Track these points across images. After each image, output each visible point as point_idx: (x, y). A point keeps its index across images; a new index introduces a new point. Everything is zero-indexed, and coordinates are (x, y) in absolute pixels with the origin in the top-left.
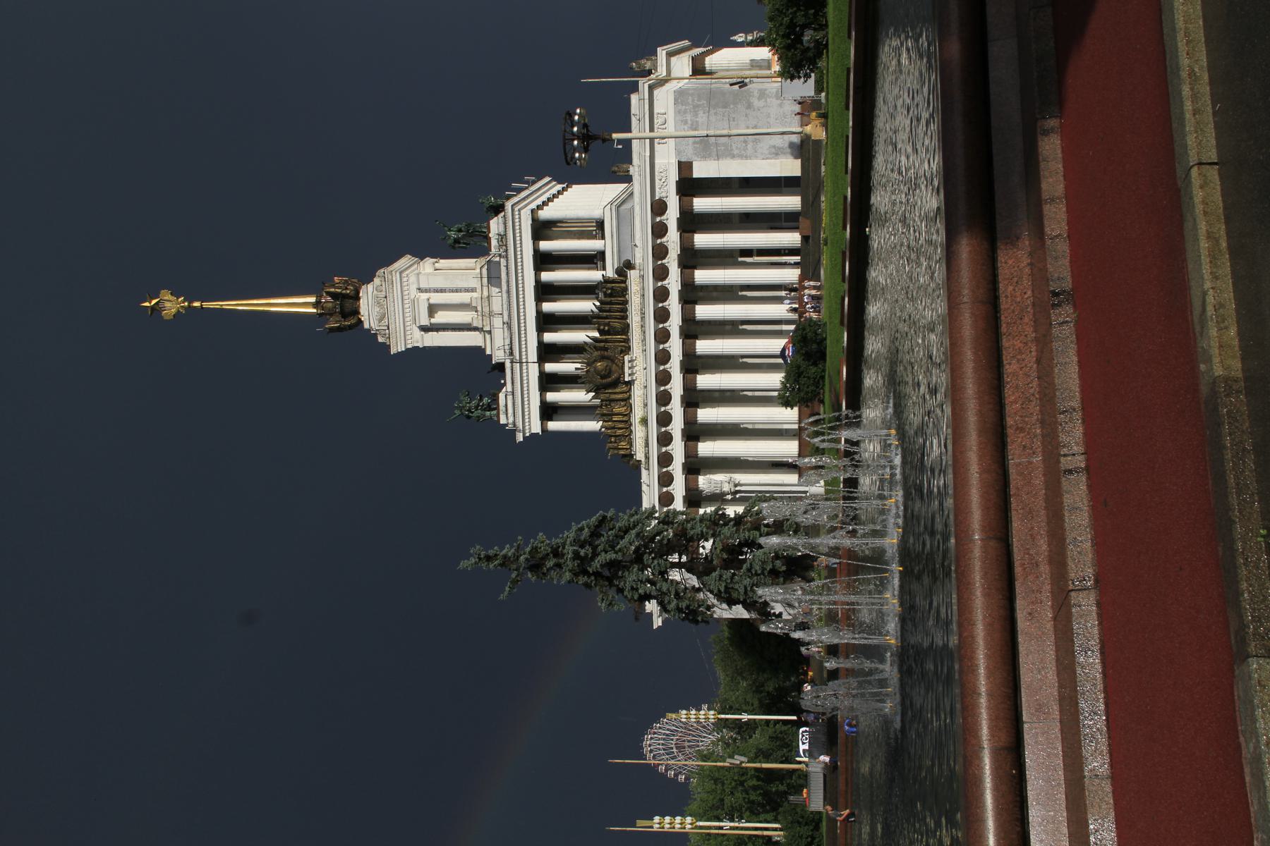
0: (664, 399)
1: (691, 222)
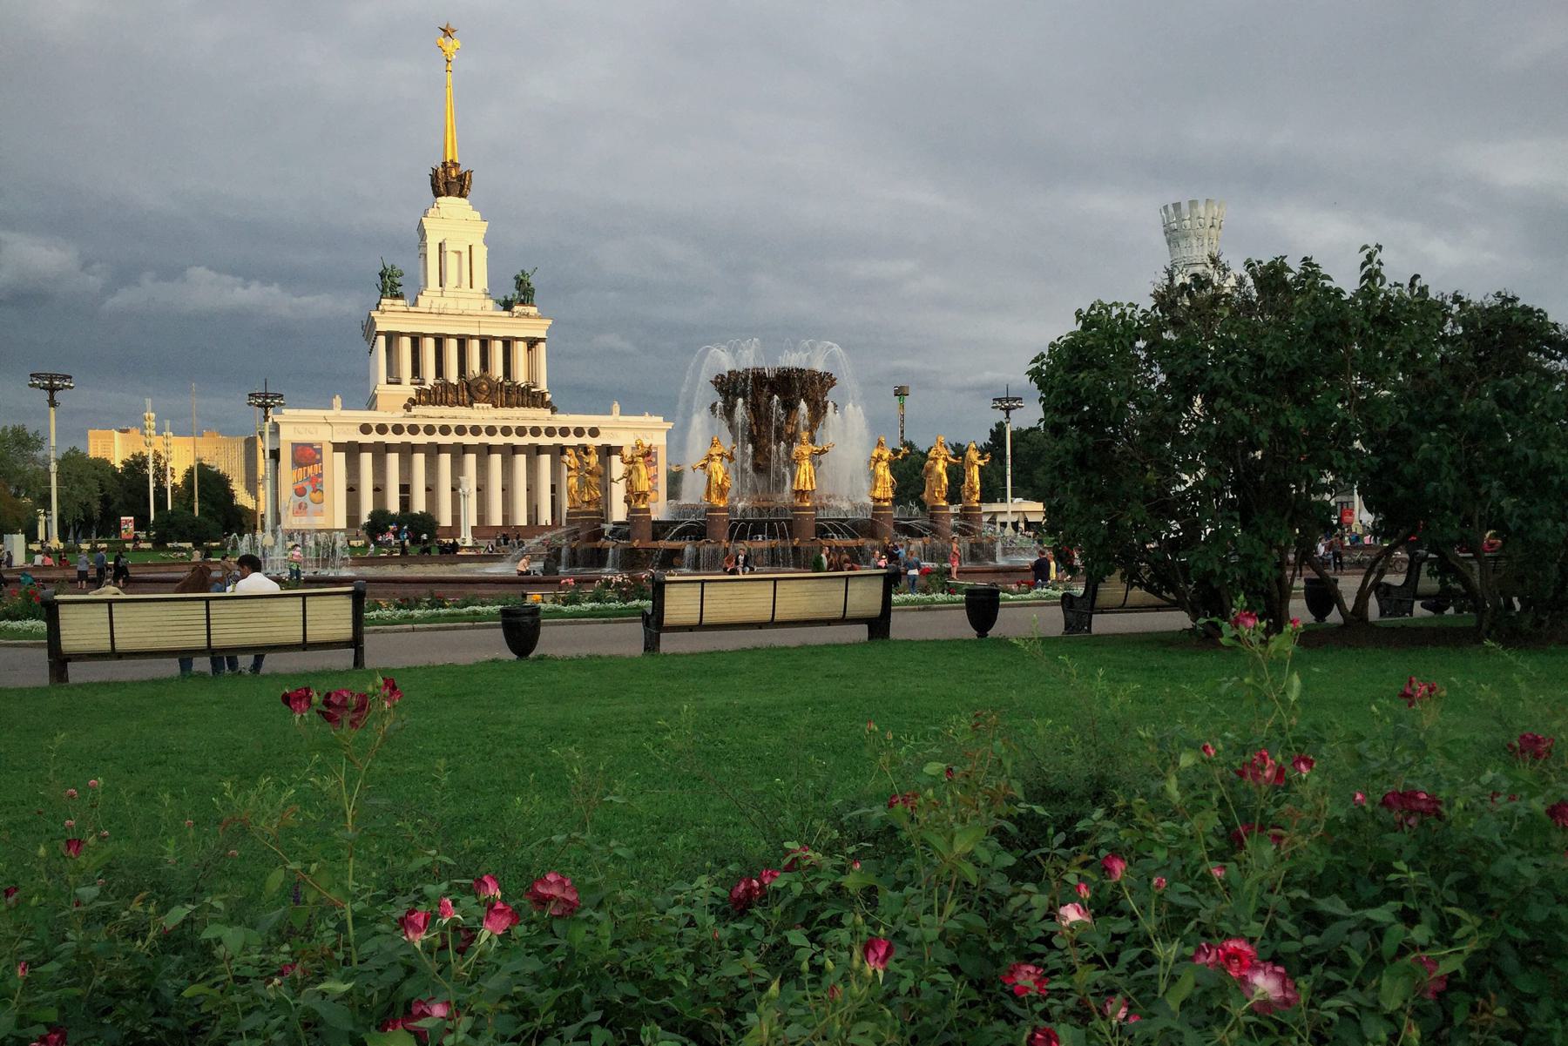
0: (461, 430)
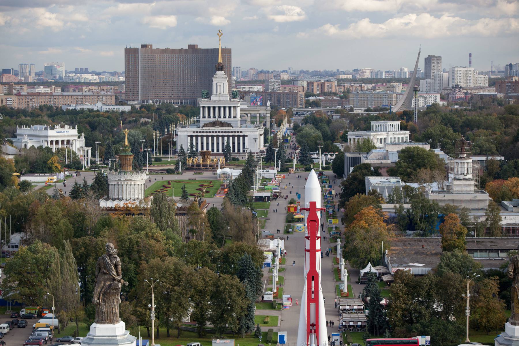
0: (213, 132)
1: (239, 136)
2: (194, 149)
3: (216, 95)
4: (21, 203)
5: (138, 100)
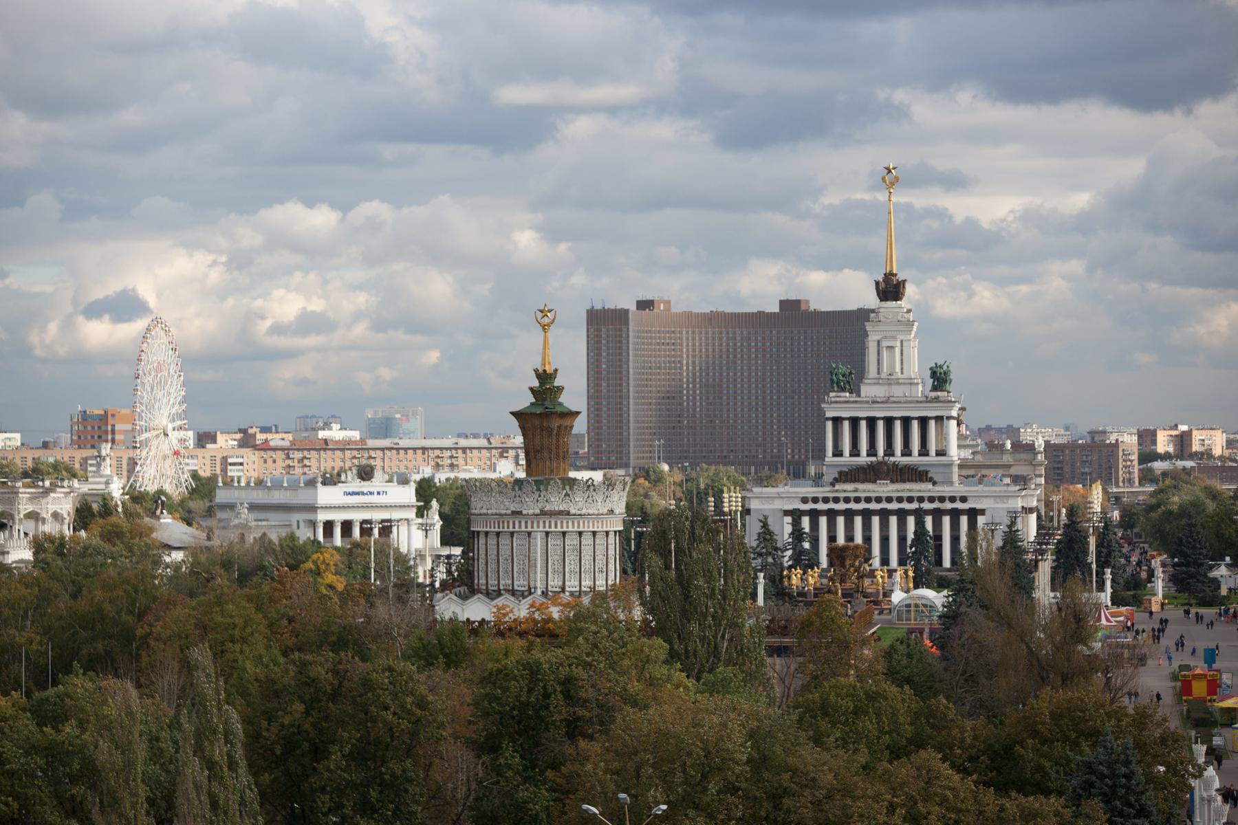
0: (868, 500)
1: (955, 514)
2: (807, 545)
3: (878, 382)
4: (107, 607)
5: (626, 466)
